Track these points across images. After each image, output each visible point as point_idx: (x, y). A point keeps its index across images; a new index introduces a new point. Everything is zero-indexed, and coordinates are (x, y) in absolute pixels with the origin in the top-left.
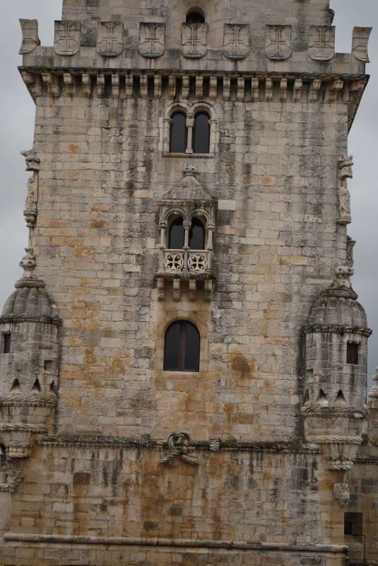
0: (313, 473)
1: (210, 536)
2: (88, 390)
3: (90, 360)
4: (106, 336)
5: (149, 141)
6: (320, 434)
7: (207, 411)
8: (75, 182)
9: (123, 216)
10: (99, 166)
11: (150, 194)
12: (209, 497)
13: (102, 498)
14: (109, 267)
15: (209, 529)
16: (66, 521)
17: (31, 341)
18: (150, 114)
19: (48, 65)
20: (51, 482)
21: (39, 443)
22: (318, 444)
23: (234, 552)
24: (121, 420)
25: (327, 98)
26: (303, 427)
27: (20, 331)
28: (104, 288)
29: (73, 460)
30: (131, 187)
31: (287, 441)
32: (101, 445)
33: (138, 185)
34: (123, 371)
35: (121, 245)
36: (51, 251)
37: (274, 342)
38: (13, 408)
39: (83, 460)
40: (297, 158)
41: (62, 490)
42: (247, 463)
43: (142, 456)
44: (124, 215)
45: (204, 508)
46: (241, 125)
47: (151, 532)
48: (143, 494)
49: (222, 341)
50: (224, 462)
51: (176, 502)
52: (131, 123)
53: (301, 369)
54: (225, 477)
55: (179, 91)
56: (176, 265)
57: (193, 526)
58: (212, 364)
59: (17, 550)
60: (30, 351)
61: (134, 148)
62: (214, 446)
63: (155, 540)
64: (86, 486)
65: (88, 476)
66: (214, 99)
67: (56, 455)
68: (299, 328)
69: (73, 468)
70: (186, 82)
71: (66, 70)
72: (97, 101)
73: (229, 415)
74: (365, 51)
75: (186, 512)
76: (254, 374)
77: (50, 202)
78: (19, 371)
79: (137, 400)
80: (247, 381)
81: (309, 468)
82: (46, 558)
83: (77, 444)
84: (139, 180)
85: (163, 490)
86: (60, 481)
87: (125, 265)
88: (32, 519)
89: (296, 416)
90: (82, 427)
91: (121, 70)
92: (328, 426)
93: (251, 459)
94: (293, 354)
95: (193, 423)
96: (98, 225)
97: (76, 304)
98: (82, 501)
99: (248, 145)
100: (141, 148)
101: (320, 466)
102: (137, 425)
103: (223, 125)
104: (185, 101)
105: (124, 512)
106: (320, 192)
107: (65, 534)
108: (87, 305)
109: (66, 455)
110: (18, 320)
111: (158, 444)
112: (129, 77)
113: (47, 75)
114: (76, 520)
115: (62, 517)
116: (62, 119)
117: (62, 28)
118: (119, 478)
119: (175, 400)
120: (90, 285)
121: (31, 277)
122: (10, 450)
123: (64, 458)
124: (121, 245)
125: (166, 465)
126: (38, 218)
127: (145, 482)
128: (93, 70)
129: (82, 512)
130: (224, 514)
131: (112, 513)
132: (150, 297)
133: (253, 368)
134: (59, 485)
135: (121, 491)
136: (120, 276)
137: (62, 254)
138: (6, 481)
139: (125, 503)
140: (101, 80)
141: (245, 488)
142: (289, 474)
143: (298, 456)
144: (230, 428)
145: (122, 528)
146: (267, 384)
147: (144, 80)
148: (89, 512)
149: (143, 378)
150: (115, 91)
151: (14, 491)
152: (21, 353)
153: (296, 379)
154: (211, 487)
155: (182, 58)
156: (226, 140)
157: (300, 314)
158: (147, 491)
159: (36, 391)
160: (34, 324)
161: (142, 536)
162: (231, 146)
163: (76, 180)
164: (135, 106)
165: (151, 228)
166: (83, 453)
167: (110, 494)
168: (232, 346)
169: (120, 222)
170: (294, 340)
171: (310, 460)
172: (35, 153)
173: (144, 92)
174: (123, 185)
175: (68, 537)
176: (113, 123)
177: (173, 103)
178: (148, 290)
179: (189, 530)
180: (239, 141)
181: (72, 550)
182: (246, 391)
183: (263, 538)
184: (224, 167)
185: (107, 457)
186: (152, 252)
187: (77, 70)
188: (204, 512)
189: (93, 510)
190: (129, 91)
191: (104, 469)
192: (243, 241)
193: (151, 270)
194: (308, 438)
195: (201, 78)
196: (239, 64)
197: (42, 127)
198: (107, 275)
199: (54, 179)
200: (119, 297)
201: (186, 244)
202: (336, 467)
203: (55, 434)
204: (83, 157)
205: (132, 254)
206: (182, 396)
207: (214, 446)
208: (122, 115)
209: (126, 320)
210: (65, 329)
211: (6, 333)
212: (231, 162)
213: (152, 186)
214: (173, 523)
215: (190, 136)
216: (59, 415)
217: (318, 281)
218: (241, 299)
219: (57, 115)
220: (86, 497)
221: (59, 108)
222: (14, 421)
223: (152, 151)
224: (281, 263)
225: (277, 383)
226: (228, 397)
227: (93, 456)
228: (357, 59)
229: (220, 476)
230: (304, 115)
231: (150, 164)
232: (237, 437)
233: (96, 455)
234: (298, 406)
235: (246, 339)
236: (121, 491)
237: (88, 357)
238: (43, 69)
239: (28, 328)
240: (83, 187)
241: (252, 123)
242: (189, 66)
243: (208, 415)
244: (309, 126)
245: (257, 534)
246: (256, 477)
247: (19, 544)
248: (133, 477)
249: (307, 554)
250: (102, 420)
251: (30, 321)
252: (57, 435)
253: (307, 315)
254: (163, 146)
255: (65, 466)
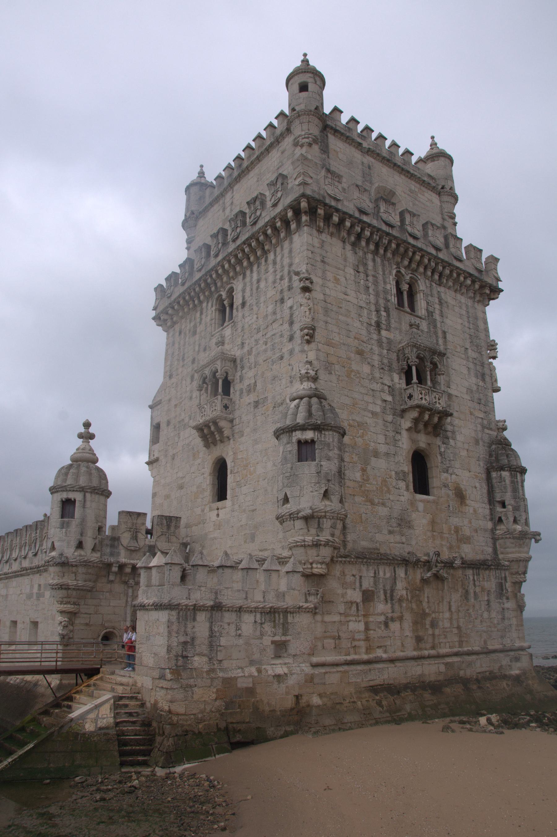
0: (505, 585)
1: (457, 644)
2: (366, 507)
3: (365, 477)
4: (375, 457)
5: (386, 292)
6: (511, 553)
7: (444, 532)
8: (340, 309)
9: (376, 349)
10: (355, 301)
11: (391, 336)
12: (453, 609)
13: (384, 615)
14: (371, 392)
15: (456, 639)
16: (359, 640)
17: (336, 451)
18: (384, 271)
19: (321, 199)
20: (345, 600)
21: (335, 559)
22: (509, 561)
23: (474, 657)
24: (391, 538)
25: (478, 298)
26: (496, 548)
27: (327, 440)
28: (369, 411)
29: (361, 577)
30: (378, 325)
31: (490, 559)
32: (383, 561)
33: (383, 326)
34: (389, 491)
35: (377, 375)
36: (328, 367)
37: (474, 476)
38: (325, 520)
39: (367, 576)
40: (468, 336)
41: (354, 608)
42: (471, 578)
43: (408, 573)
44: (377, 348)
45: (451, 619)
46: (437, 301)
47: (422, 645)
48: (412, 609)
49: (447, 471)
50: (459, 578)
51: (433, 615)
52: (373, 273)
53: (491, 501)
54: (460, 590)
55: (403, 256)
56: (426, 400)
57: (446, 637)
58: (444, 491)
59: (327, 676)
60: (336, 461)
61: (377, 295)
62: (458, 562)
63: (426, 653)
64: (372, 604)
65: (373, 592)
66: (421, 274)
67: (346, 571)
68: (485, 467)
69: (361, 586)
70: (410, 254)
71: (337, 210)
72: (348, 247)
73: (457, 535)
74: (497, 273)
75: (440, 623)
76: (468, 502)
77: (324, 321)
78: (329, 481)
79: (401, 519)
80: (464, 507)
81: (503, 581)
82: (351, 681)
83: (365, 560)
84: (384, 322)
85: (425, 604)
86: (352, 599)
87: (381, 393)
88: (332, 641)
89: (492, 539)
90: (364, 544)
91: (374, 227)
92: (520, 546)
93: (474, 574)
94: (485, 486)
95: (438, 542)
96: (360, 353)
97: (351, 422)
98: (371, 619)
99: (442, 316)
100: (382, 296)
101: (508, 579)
102: (403, 543)
103: (427, 296)
104: (404, 269)
105: (401, 628)
106: (482, 365)
107: (360, 654)
108: (361, 425)
109: (354, 573)
110: (326, 427)
111: (421, 561)
112: (377, 235)
113: (321, 209)
114: (367, 639)
115: (357, 636)
116: (327, 252)
117: (330, 176)
118: (395, 594)
119: (425, 521)
120: (360, 406)
121: (316, 389)
122: (314, 565)
123: (354, 576)
124: (377, 375)
125: (424, 581)
126: (316, 333)
127: (412, 597)
128: (356, 218)
129: (371, 630)
130: (461, 624)
131: (392, 630)
132: (400, 426)
133: (466, 497)
134: (352, 603)
135: (397, 606)
136: (379, 402)
137: (337, 373)
138: (306, 601)
139: (401, 618)
140: (358, 229)
141: (472, 600)
142: (494, 586)
143: (497, 572)
144: (459, 547)
145: (400, 644)
146: (475, 511)
147: (385, 241)
148: (377, 629)
149: (402, 499)
150: (363, 243)
151: (314, 611)
152: (329, 462)
153: (488, 507)
154: (453, 600)
155: (407, 234)
156: (431, 309)
157: (484, 456)
158: (414, 606)
159: (340, 505)
160: (337, 435)
161: (415, 650)
162: (434, 314)
163: (341, 308)
164: (374, 260)
165: (395, 365)
166: (368, 570)
167: (390, 611)
168: (454, 476)
169: (374, 354)
170: (484, 476)
171: (503, 576)
172: (309, 274)
173: (381, 251)
174: (373, 322)
175: (365, 657)
176: (361, 269)
177: (396, 268)
178: (399, 418)
179: (444, 641)
180: (437, 312)
181: (370, 670)
182: (464, 516)
183: (485, 642)
184: (432, 329)
185: (385, 574)
186: (398, 386)
187: (345, 213)
188: (451, 624)
189: (380, 628)
190: (372, 247)
191: (384, 586)
192: (451, 391)
193: (399, 401)
194: (501, 556)
195: (420, 254)
196: (439, 253)
197: (312, 253)
198: (370, 399)
199: (325, 301)
200: (380, 422)
201: (429, 383)
202: (521, 579)
203: (345, 550)
204: (343, 289)
205: (386, 385)
206: (429, 516)
207: (458, 562)
208: (366, 264)
209: (387, 444)
210: (345, 444)
211: (306, 442)
212: (435, 327)
213: (392, 330)
214: (433, 635)
215: (407, 297)
216: (347, 531)
217: (490, 432)
218: (454, 439)
219: (322, 247)
220: (372, 615)
221: (323, 241)
222: (324, 533)
223: (389, 301)
224: (471, 414)
225: (480, 510)
226: (455, 521)
227: (375, 573)
228: (494, 276)
229: (457, 590)
230: (467, 305)
231: (389, 311)
232: (464, 556)
233: (377, 572)
234: (493, 530)
235: (459, 472)
236: (397, 606)
237: (363, 474)
238: (318, 201)
239: (333, 438)
240: (346, 316)
241: (442, 301)
242: (411, 241)
243: (445, 535)
244: (470, 314)
245: (483, 639)
246: (478, 590)
247: (327, 669)
248: (404, 592)
249: (512, 653)
250: (379, 537)
251: (335, 431)
252: (347, 550)
253: (488, 457)
254: (394, 300)
255: (355, 583)
